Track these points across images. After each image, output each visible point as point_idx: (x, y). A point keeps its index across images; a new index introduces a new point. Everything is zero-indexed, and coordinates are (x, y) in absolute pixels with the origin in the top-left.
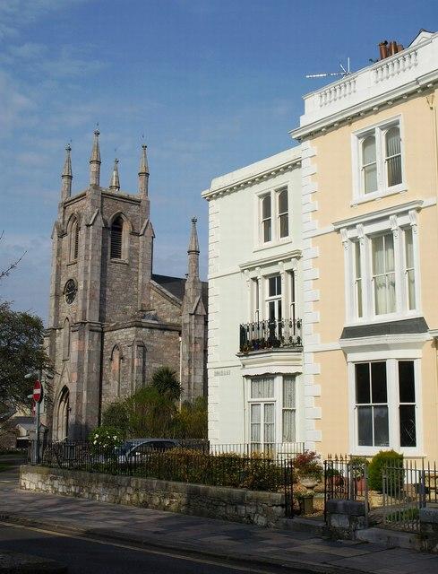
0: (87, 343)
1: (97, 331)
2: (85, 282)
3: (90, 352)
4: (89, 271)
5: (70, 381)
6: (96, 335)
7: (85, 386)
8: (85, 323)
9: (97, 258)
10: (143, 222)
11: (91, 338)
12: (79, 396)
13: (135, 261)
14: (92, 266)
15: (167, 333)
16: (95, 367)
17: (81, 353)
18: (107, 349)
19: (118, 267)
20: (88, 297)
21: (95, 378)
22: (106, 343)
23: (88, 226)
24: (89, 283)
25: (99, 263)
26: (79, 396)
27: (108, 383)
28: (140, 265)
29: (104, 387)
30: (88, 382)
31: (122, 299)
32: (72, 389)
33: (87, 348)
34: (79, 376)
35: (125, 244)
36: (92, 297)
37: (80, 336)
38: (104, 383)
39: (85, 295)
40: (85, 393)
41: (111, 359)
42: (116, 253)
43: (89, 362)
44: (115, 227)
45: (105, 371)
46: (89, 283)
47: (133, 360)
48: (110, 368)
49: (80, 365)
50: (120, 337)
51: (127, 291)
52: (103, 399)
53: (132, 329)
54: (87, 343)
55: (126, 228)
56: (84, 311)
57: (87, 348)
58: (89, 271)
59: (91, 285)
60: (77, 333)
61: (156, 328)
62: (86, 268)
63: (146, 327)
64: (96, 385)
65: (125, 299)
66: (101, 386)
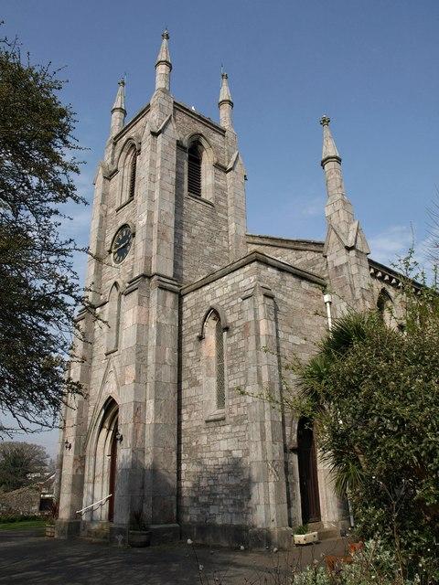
0: (154, 311)
1: (172, 291)
2: (150, 214)
3: (159, 325)
4: (156, 196)
5: (120, 384)
6: (171, 298)
7: (150, 390)
8: (150, 278)
9: (169, 180)
10: (230, 156)
11: (162, 302)
12: (139, 409)
13: (222, 203)
14: (162, 189)
15: (305, 285)
16: (169, 355)
17: (142, 328)
18: (192, 319)
19: (200, 206)
20: (155, 236)
21: (169, 374)
22: (187, 313)
23: (155, 134)
24: (156, 215)
25: (172, 188)
26: (139, 409)
27: (196, 383)
28: (231, 210)
29: (188, 392)
30: (157, 382)
31: (206, 253)
32: (125, 400)
33: (153, 318)
34: (138, 372)
35: (208, 178)
36: (162, 235)
37: (140, 297)
38: (185, 385)
39: (149, 233)
40: (151, 405)
41: (201, 338)
42: (195, 188)
43: (158, 344)
44: (192, 152)
45: (187, 363)
46: (156, 215)
47: (257, 323)
48: (199, 354)
49: (140, 351)
50: (219, 293)
51: (213, 244)
52: (185, 417)
53: (247, 268)
54: (154, 311)
55: (207, 160)
56: (148, 259)
57: (153, 318)
58: (156, 196)
59: (160, 217)
60: (135, 294)
61: (288, 272)
62: (151, 193)
63: (273, 267)
64: (172, 389)
65: (212, 254)
66: (179, 391)
